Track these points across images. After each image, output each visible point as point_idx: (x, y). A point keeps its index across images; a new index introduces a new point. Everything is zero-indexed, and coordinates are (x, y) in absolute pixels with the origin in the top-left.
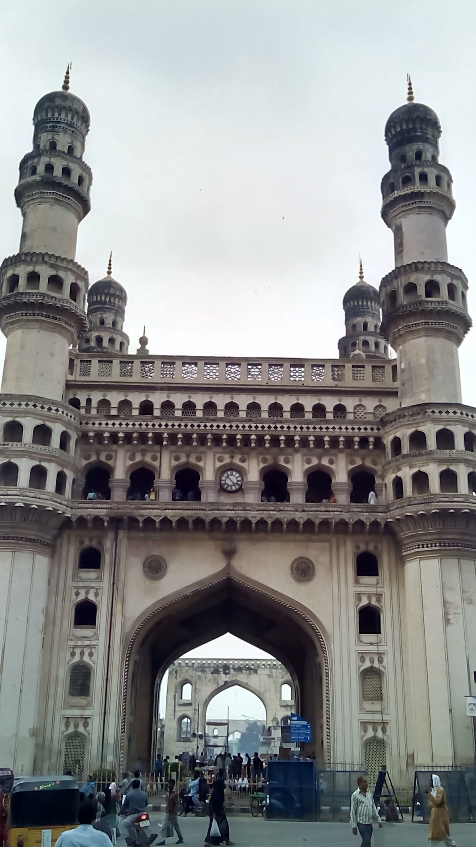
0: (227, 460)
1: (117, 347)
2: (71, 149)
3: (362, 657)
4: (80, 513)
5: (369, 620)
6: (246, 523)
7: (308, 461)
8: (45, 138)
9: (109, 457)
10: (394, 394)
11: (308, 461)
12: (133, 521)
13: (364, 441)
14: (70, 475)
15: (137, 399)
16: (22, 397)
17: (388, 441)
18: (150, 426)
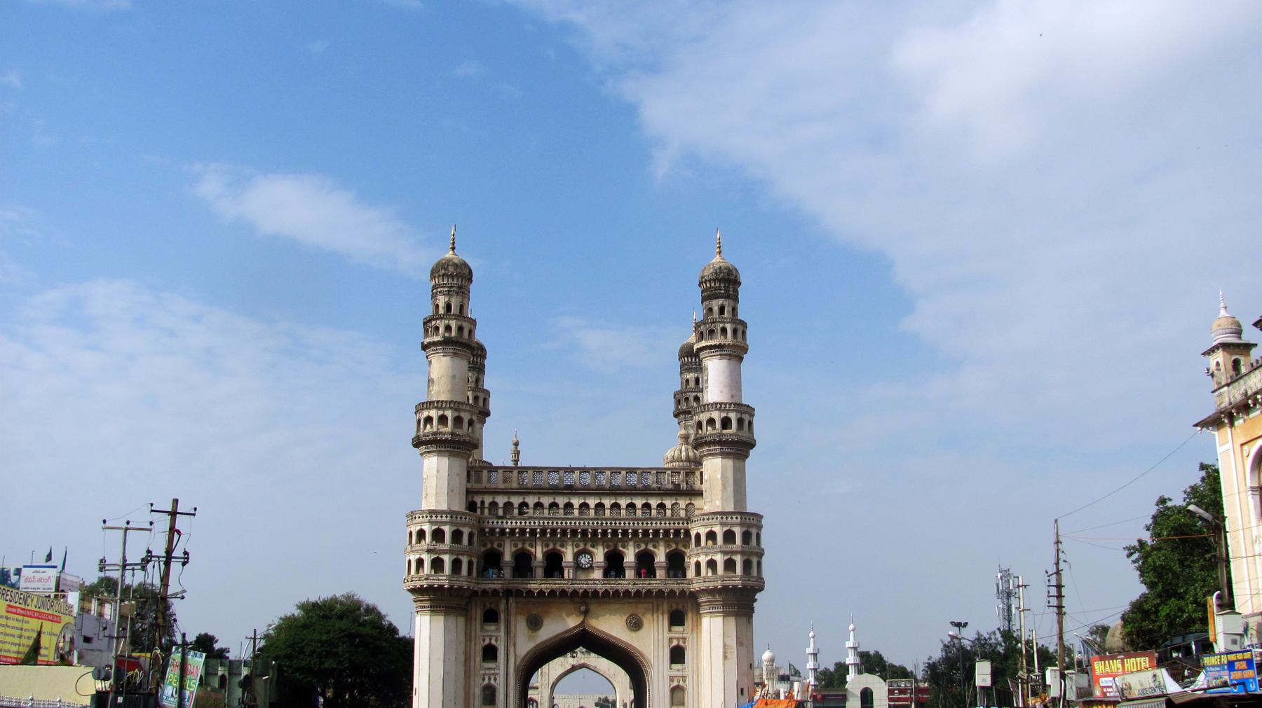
0: (582, 546)
1: (481, 403)
2: (462, 307)
3: (672, 678)
4: (483, 587)
5: (677, 655)
6: (596, 592)
7: (639, 546)
8: (442, 301)
9: (500, 545)
10: (700, 494)
11: (639, 546)
12: (519, 593)
13: (677, 532)
14: (475, 560)
15: (516, 501)
16: (442, 512)
17: (693, 533)
18: (527, 525)
